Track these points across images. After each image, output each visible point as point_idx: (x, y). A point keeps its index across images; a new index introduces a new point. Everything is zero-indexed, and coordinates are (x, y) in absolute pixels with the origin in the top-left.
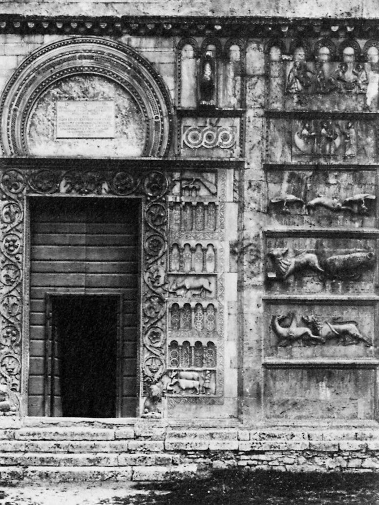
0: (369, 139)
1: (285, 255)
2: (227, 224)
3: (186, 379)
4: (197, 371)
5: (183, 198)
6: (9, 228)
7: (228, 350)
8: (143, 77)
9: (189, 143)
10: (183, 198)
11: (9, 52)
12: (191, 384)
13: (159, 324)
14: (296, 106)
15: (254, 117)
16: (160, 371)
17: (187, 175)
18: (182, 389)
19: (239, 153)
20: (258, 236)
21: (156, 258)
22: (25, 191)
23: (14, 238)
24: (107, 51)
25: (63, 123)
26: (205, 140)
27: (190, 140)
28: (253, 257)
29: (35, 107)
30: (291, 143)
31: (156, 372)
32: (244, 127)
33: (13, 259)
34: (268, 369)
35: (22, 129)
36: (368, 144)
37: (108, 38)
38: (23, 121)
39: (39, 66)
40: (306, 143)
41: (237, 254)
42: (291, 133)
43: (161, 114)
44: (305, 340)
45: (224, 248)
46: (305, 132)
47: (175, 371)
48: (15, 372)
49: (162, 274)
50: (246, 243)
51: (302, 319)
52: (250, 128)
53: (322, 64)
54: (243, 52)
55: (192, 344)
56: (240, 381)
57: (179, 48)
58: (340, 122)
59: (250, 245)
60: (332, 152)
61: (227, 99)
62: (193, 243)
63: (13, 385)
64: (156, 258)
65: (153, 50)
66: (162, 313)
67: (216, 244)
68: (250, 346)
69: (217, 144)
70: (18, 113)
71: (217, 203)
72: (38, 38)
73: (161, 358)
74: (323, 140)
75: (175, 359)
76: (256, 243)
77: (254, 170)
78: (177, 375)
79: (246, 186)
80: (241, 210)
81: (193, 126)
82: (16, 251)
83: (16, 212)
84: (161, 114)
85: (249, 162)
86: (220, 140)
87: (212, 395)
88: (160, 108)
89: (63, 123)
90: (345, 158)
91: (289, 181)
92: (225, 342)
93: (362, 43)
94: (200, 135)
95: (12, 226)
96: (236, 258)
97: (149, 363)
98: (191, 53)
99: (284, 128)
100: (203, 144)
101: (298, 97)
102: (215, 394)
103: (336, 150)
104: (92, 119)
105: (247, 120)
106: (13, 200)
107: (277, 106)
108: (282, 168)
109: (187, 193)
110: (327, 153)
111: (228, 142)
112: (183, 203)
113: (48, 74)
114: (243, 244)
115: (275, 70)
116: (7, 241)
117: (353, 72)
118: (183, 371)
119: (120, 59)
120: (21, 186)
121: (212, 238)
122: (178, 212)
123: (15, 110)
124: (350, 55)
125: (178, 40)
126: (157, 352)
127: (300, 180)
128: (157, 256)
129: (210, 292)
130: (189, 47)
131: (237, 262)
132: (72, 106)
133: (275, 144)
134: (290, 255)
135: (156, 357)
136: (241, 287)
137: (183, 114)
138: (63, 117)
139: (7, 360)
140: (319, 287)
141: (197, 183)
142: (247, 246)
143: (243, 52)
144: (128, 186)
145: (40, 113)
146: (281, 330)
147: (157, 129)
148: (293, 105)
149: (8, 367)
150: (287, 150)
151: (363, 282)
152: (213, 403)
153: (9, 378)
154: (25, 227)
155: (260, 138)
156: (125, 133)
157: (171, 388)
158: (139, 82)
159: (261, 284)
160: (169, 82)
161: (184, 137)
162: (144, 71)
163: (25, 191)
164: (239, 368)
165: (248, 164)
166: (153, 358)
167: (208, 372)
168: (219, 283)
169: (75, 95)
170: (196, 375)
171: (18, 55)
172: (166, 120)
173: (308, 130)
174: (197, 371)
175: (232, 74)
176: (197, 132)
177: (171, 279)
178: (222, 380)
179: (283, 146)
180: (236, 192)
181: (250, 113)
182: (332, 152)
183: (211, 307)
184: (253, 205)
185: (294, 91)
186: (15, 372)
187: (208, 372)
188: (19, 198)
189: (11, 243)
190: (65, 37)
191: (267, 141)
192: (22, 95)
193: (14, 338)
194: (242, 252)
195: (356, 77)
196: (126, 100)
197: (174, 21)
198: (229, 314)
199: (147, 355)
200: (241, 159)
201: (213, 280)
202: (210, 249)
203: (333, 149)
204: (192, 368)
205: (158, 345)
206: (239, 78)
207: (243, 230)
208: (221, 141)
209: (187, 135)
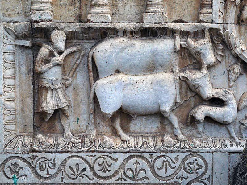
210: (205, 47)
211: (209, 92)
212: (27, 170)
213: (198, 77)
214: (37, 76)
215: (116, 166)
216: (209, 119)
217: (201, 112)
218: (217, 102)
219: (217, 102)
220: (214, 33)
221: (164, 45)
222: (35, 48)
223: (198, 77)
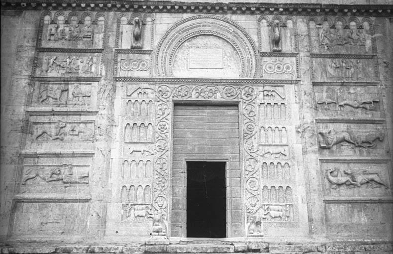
0: (370, 69)
1: (329, 133)
2: (293, 116)
3: (274, 210)
4: (281, 205)
5: (265, 101)
6: (161, 118)
8: (239, 36)
10: (265, 101)
11: (164, 22)
12: (277, 214)
13: (255, 176)
14: (344, 33)
16: (258, 205)
17: (267, 88)
18: (272, 218)
19: (297, 76)
20: (313, 122)
21: (252, 135)
22: (171, 97)
23: (164, 123)
24: (218, 23)
26: (276, 69)
27: (268, 69)
28: (311, 134)
29: (177, 51)
30: (326, 72)
31: (255, 206)
33: (163, 136)
34: (326, 203)
35: (221, 8)
36: (370, 72)
37: (219, 15)
39: (180, 30)
40: (335, 71)
42: (325, 66)
43: (251, 55)
44: (347, 184)
45: (292, 129)
47: (267, 205)
48: (164, 207)
49: (256, 145)
50: (306, 126)
51: (344, 171)
53: (338, 30)
54: (295, 23)
55: (277, 188)
56: (309, 211)
57: (259, 21)
58: (352, 60)
59: (309, 127)
60: (350, 76)
61: (287, 46)
62: (273, 126)
63: (163, 215)
64: (252, 135)
66: (256, 169)
67: (288, 127)
69: (284, 71)
70: (168, 54)
71: (286, 104)
72: (180, 15)
73: (257, 197)
74: (344, 69)
76: (312, 126)
77: (306, 83)
78: (268, 208)
81: (269, 62)
82: (165, 131)
83: (166, 109)
84: (251, 55)
86: (285, 69)
87: (292, 222)
88: (250, 52)
90: (358, 79)
91: (327, 92)
93: (360, 19)
94: (273, 66)
95: (163, 116)
96: (300, 135)
97: (250, 200)
98: (266, 24)
99: (321, 62)
100: (275, 71)
102: (293, 221)
103: (352, 75)
107: (316, 51)
108: (321, 84)
109: (267, 98)
110: (348, 76)
111: (290, 70)
113: (185, 34)
115: (313, 33)
116: (160, 126)
117: (357, 34)
118: (272, 205)
119: (225, 27)
120: (169, 94)
122: (263, 109)
123: (166, 53)
124: (354, 26)
125: (259, 16)
126: (255, 193)
127: (333, 91)
128: (251, 134)
129: (285, 155)
130: (264, 21)
132: (198, 51)
133: (317, 71)
134: (332, 133)
135: (254, 196)
137: (263, 55)
139: (158, 199)
140: (351, 153)
141: (273, 92)
142: (307, 128)
143: (295, 23)
144: (232, 94)
145: (180, 54)
146: (331, 178)
147: (249, 62)
148: (325, 51)
149: (159, 203)
150: (324, 75)
151: (378, 150)
152: (293, 226)
153: (160, 211)
154: (170, 117)
156: (229, 66)
157: (265, 217)
158: (237, 38)
159: (317, 150)
160: (255, 38)
161: (264, 68)
162: (239, 33)
163: (171, 97)
166: (252, 197)
167: (288, 206)
169: (200, 46)
170: (280, 208)
172: (253, 58)
174: (281, 205)
175: (289, 35)
176: (271, 65)
177: (261, 148)
178: (297, 211)
179: (322, 73)
181: (302, 54)
182: (350, 76)
183: (287, 165)
185: (325, 44)
186: (164, 207)
187: (288, 206)
188: (167, 101)
189: (163, 127)
190: (196, 15)
192: (170, 45)
193: (163, 185)
194: (304, 131)
195: (358, 37)
196: (229, 48)
197: (257, 6)
198: (298, 169)
199: (249, 195)
200: (298, 79)
201: (286, 148)
203: (350, 74)
204: (278, 203)
205: (256, 189)
206: (293, 37)
209: (266, 66)
210: (149, 206)
223: (149, 211)
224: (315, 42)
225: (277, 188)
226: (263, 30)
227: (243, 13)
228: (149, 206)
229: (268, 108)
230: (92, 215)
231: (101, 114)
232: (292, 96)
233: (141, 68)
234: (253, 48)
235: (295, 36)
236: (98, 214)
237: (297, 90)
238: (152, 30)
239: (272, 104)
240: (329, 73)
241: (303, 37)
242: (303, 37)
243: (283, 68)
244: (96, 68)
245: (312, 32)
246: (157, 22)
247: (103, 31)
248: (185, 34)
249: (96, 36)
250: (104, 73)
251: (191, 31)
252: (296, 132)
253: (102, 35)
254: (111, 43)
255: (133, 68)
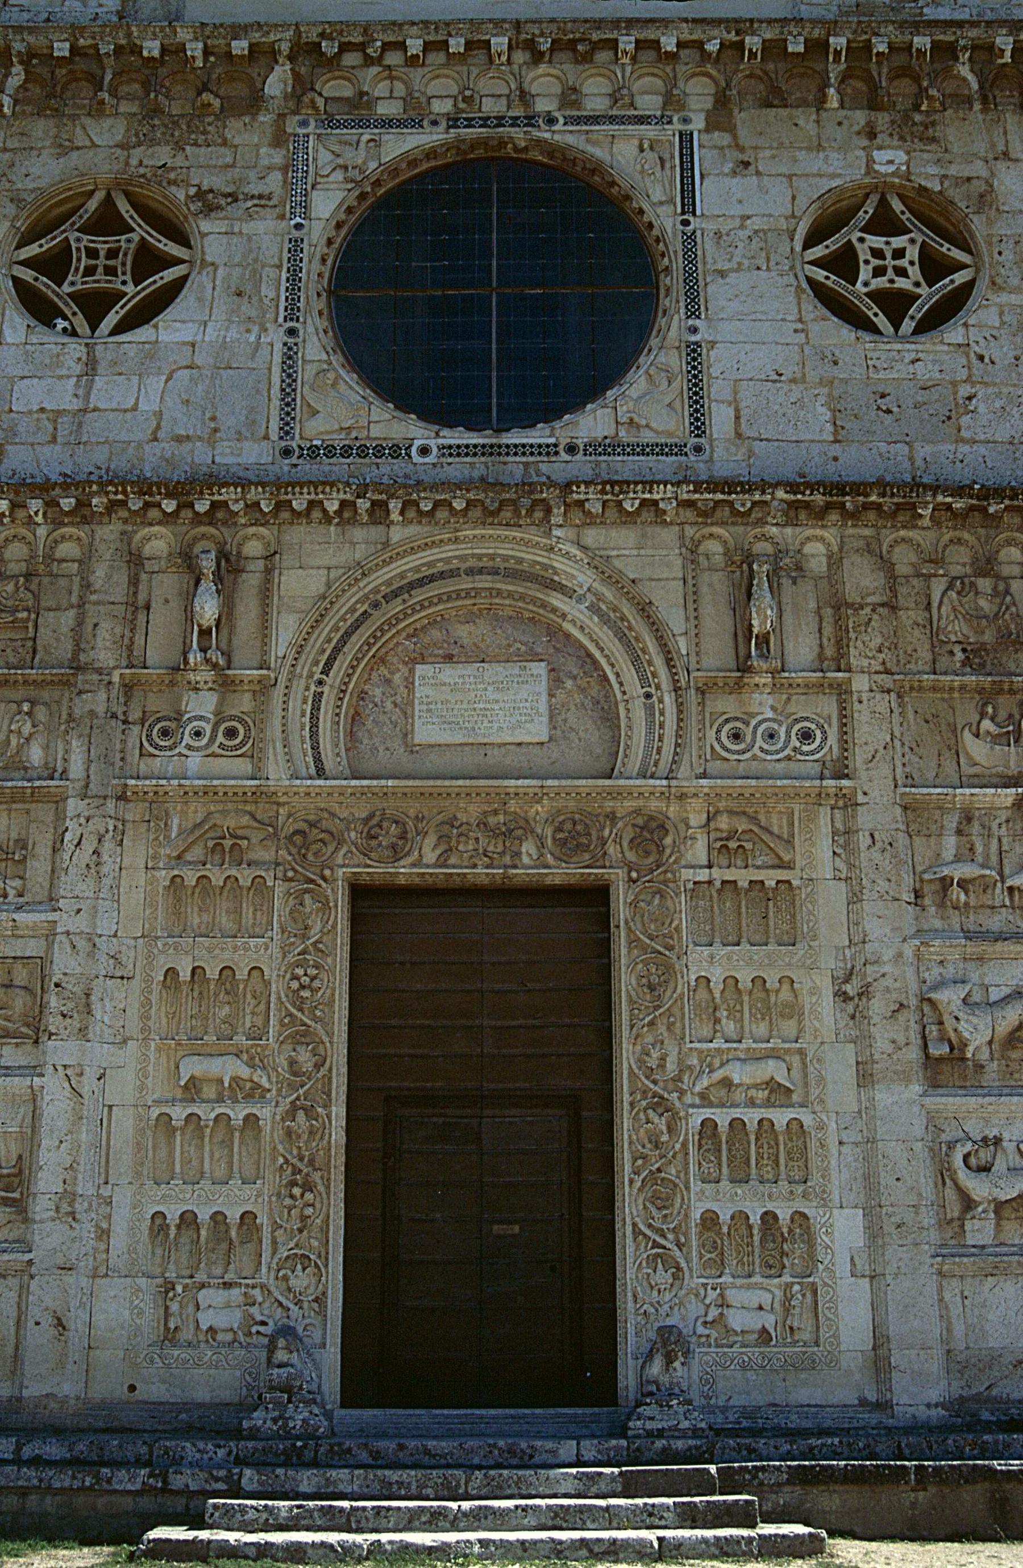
7: (843, 1231)
9: (727, 750)
15: (871, 691)
25: (429, 711)
32: (848, 713)
38: (340, 699)
41: (852, 999)
46: (987, 724)
52: (862, 714)
65: (635, 552)
68: (896, 1219)
70: (326, 689)
71: (795, 883)
75: (713, 1255)
76: (897, 973)
79: (864, 840)
80: (855, 898)
85: (865, 789)
86: (795, 742)
89: (429, 711)
92: (835, 1211)
100: (756, 750)
101: (964, 650)
104: (497, 701)
105: (855, 697)
106: (312, 881)
112: (718, 884)
114: (865, 976)
121: (790, 964)
123: (320, 683)
131: (853, 1017)
136: (865, 1077)
138: (427, 697)
143: (835, 561)
155: (888, 738)
160: (675, 621)
164: (872, 1277)
165: (865, 794)
168: (811, 1069)
171: (329, 568)
173: (992, 719)
176: (739, 724)
180: (839, 855)
184: (882, 885)
191: (903, 744)
194: (865, 993)
202: (786, 986)
207: (864, 942)
208: (798, 744)
209: (718, 731)
211: (259, 1318)
212: (158, 1360)
213: (254, 1310)
214: (167, 1308)
215: (206, 1359)
216: (258, 1332)
217: (254, 1330)
218: (264, 1323)
219: (264, 1323)
220: (263, 1286)
221: (235, 1292)
222: (167, 1293)
223: (254, 1310)
224: (917, 633)
225: (755, 1219)
226: (710, 585)
227: (628, 518)
228: (257, 1292)
229: (728, 904)
230: (37, 1324)
231: (68, 933)
232: (824, 848)
233: (221, 746)
234: (669, 662)
235: (837, 608)
236: (59, 1319)
237: (839, 825)
238: (266, 593)
239: (740, 884)
240: (967, 753)
241: (868, 610)
242: (868, 610)
243: (788, 733)
244: (46, 747)
245: (903, 590)
246: (288, 559)
247: (74, 600)
248: (396, 607)
249: (48, 618)
250: (77, 769)
251: (420, 595)
252: (835, 995)
253: (68, 618)
254: (104, 652)
255: (189, 747)
